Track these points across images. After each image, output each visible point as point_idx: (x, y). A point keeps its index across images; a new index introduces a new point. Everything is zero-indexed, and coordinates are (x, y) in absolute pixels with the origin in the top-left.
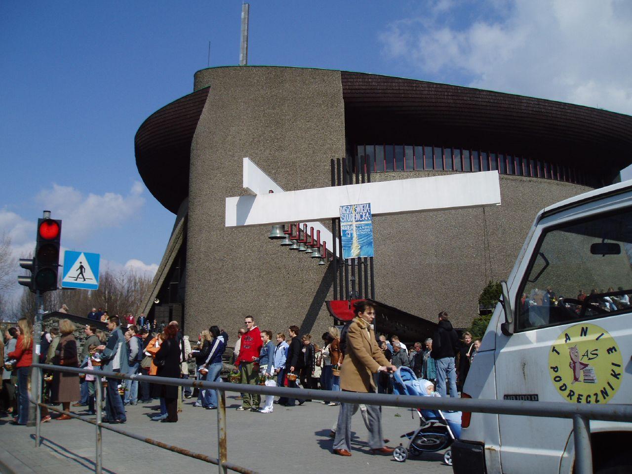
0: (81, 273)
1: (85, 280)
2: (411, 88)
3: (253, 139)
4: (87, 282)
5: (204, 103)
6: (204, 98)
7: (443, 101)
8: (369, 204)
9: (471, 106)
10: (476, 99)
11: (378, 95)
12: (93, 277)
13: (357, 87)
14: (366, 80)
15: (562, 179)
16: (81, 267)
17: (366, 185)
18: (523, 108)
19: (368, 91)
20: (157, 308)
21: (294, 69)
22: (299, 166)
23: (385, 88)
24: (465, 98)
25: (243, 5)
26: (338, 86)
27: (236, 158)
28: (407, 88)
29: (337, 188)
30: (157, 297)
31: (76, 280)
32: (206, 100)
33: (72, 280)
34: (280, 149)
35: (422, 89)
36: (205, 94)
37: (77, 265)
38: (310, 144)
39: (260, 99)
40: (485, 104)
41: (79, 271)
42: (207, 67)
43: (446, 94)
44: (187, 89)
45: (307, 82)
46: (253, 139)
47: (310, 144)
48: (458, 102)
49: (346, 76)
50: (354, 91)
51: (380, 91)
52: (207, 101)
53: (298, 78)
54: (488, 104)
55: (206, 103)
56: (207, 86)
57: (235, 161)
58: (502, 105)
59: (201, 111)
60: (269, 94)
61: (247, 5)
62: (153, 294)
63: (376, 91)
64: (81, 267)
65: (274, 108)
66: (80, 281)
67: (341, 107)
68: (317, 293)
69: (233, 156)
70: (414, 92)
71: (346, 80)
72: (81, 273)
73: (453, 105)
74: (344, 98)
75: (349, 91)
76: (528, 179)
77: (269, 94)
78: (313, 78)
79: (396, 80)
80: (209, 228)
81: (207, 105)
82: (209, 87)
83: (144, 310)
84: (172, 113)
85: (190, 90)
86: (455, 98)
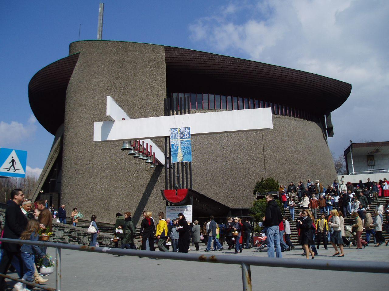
0: (13, 165)
1: (15, 171)
2: (208, 58)
3: (108, 87)
4: (17, 172)
5: (76, 63)
6: (75, 60)
7: (227, 66)
8: (189, 128)
9: (244, 71)
10: (247, 66)
11: (187, 62)
12: (22, 168)
13: (174, 56)
14: (180, 52)
15: (297, 117)
16: (13, 161)
17: (187, 115)
18: (276, 73)
19: (181, 59)
20: (42, 195)
22: (137, 105)
23: (192, 57)
24: (241, 66)
25: (100, 4)
26: (162, 55)
27: (96, 99)
28: (206, 58)
29: (168, 117)
30: (42, 189)
31: (9, 170)
32: (77, 61)
33: (5, 171)
35: (215, 59)
36: (76, 57)
37: (9, 159)
38: (144, 91)
40: (253, 69)
41: (11, 164)
42: (78, 40)
43: (229, 62)
44: (65, 54)
45: (143, 52)
46: (108, 87)
47: (144, 91)
48: (237, 67)
49: (168, 49)
50: (172, 59)
51: (189, 59)
52: (77, 62)
53: (137, 49)
54: (255, 70)
55: (77, 63)
56: (78, 52)
57: (95, 101)
58: (263, 71)
59: (74, 68)
60: (118, 58)
61: (103, 4)
62: (39, 187)
63: (186, 59)
64: (13, 161)
65: (121, 68)
66: (12, 171)
68: (148, 185)
70: (210, 61)
71: (167, 52)
72: (13, 165)
73: (234, 70)
74: (166, 63)
75: (169, 59)
76: (278, 116)
77: (118, 58)
78: (146, 50)
79: (199, 53)
80: (78, 143)
81: (77, 65)
83: (33, 197)
85: (66, 55)
86: (235, 65)
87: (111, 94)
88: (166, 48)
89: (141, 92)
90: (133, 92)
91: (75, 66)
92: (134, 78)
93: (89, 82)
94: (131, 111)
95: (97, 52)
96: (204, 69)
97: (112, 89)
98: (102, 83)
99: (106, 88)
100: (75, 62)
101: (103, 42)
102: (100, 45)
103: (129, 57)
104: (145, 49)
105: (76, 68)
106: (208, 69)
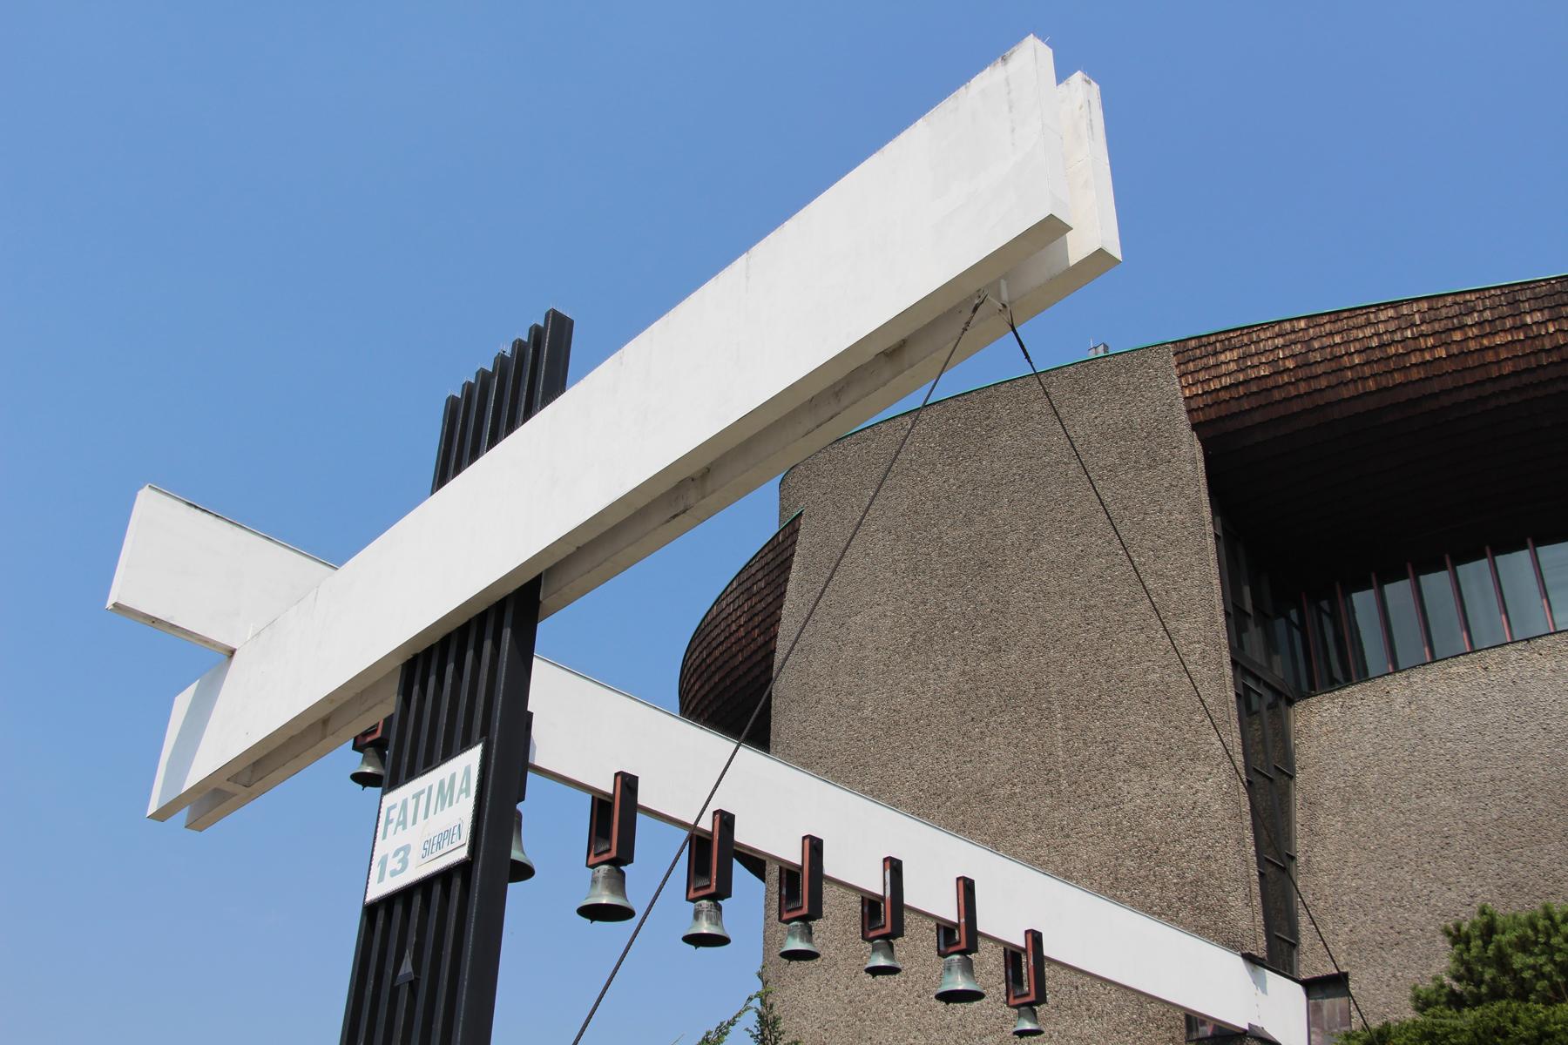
21: (1021, 381)
32: (793, 555)
34: (996, 647)
38: (1087, 608)
39: (929, 505)
52: (795, 559)
57: (863, 720)
59: (783, 594)
65: (968, 521)
67: (1191, 451)
69: (858, 708)
74: (1194, 427)
77: (952, 481)
78: (1083, 392)
81: (793, 575)
82: (801, 514)
84: (723, 625)
87: (931, 666)
88: (1182, 348)
89: (1077, 618)
90: (1036, 628)
91: (787, 580)
92: (1033, 553)
93: (835, 638)
94: (1030, 734)
95: (861, 483)
96: (1434, 395)
97: (931, 639)
98: (889, 622)
99: (910, 644)
100: (786, 565)
101: (884, 427)
102: (873, 446)
103: (999, 458)
104: (1072, 391)
105: (790, 586)
106: (1457, 389)
